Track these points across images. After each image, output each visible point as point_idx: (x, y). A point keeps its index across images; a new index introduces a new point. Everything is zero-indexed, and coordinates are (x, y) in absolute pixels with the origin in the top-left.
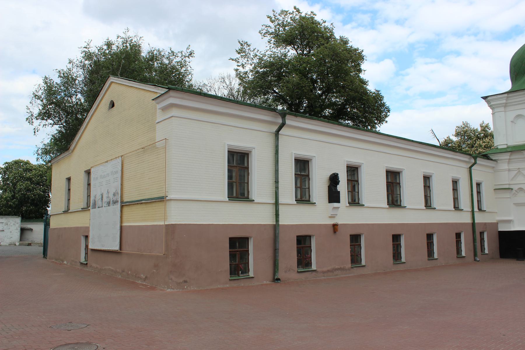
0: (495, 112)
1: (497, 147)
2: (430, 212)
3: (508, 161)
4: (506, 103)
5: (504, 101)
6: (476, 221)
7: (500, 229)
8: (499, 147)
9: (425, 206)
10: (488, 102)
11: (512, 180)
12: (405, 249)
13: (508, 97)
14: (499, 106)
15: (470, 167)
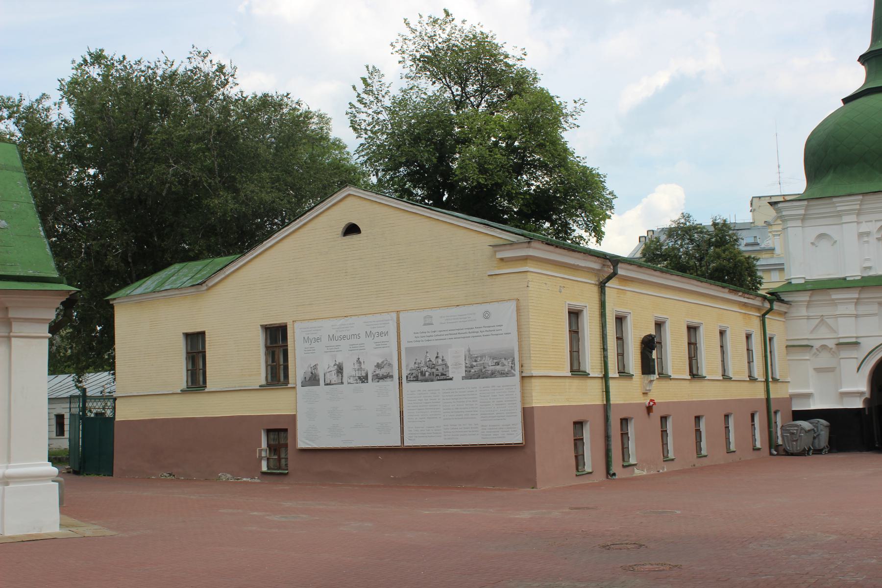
0: (788, 226)
1: (790, 281)
2: (697, 385)
3: (806, 303)
5: (802, 212)
6: (772, 396)
7: (795, 408)
8: (794, 282)
9: (722, 376)
10: (778, 211)
11: (812, 332)
12: (706, 438)
13: (807, 206)
14: (793, 218)
15: (764, 315)
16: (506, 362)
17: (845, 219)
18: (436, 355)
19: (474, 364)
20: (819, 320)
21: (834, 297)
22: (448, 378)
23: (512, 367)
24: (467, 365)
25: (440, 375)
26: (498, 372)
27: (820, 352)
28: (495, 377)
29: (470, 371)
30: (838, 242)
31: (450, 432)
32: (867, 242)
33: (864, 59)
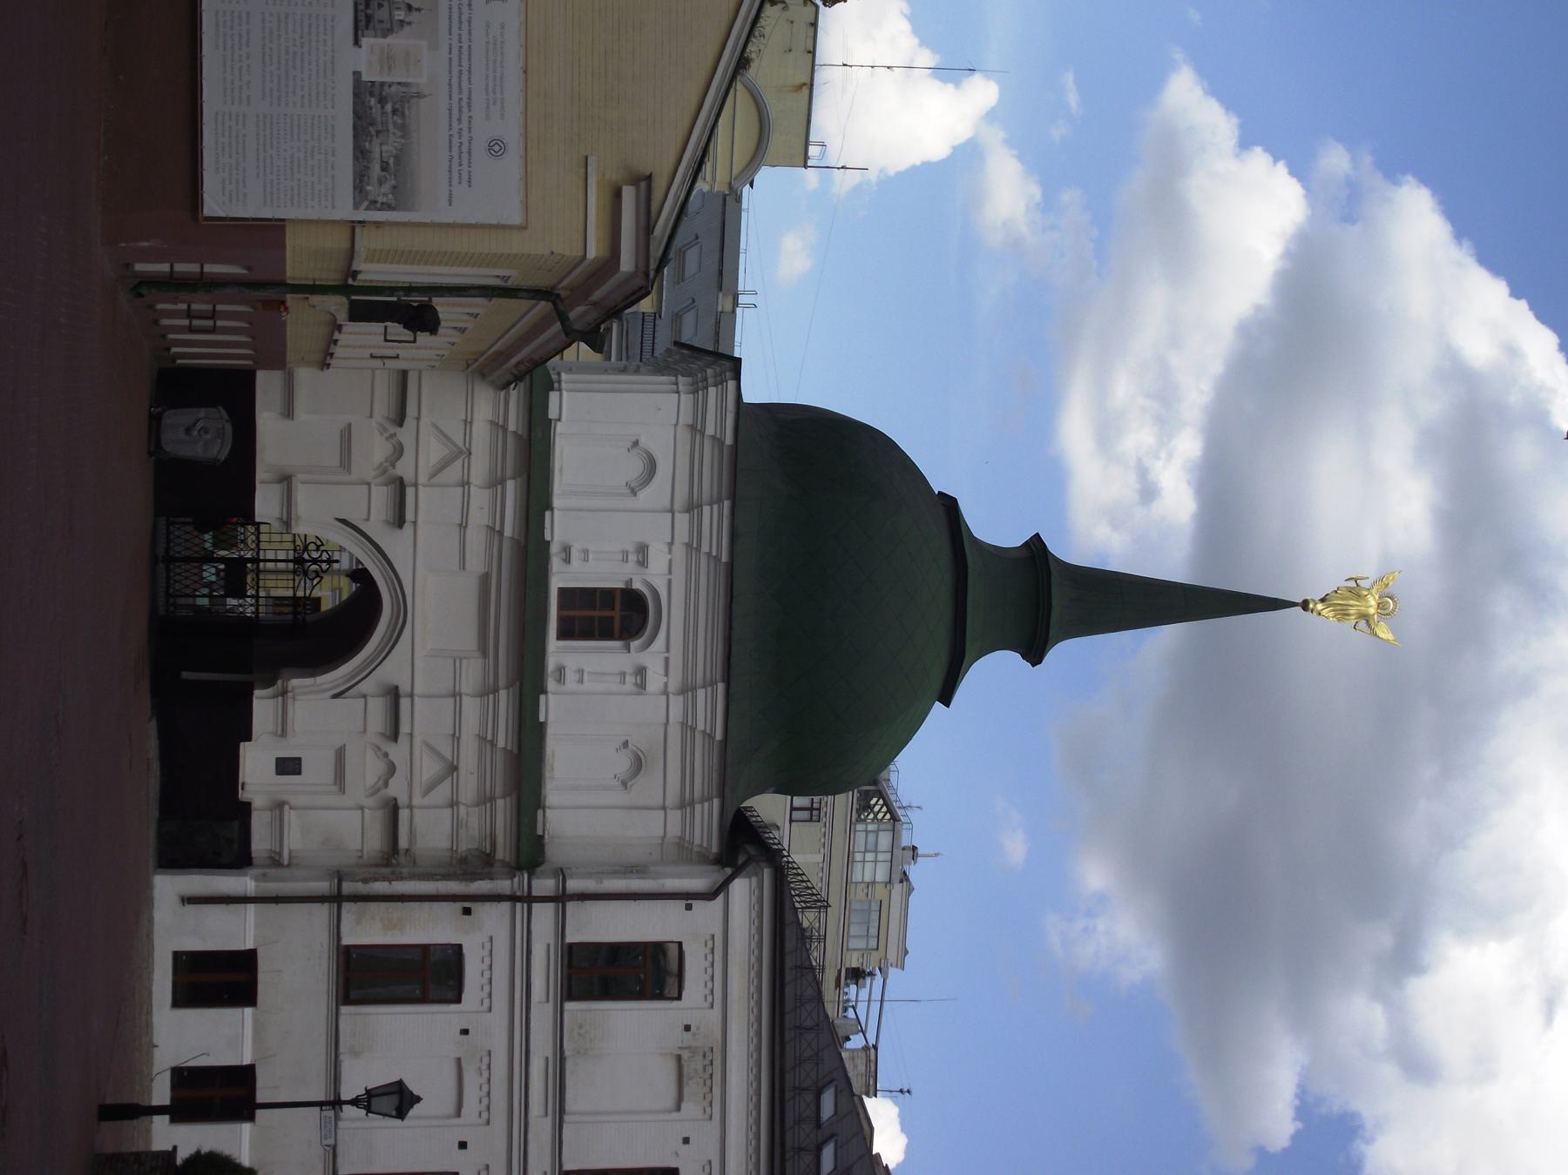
1: (556, 385)
3: (501, 423)
4: (702, 433)
7: (262, 377)
8: (553, 396)
16: (386, 188)
17: (682, 520)
18: (415, 5)
19: (389, 107)
20: (460, 444)
21: (510, 485)
22: (360, 32)
23: (376, 202)
24: (386, 88)
25: (369, 12)
26: (367, 168)
27: (387, 439)
28: (356, 158)
29: (372, 94)
31: (232, 28)
33: (1036, 545)
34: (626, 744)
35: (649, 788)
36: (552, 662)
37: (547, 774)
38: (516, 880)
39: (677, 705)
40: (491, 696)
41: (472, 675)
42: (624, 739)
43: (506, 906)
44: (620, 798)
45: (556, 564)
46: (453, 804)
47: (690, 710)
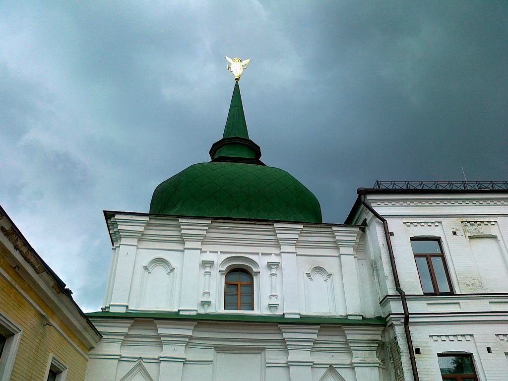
17: (188, 244)
20: (135, 364)
30: (175, 271)
32: (209, 273)
34: (308, 275)
35: (330, 264)
36: (266, 312)
37: (328, 315)
38: (394, 323)
39: (284, 248)
40: (287, 343)
41: (274, 356)
42: (305, 275)
43: (411, 328)
44: (336, 278)
45: (211, 310)
46: (352, 367)
47: (288, 241)
